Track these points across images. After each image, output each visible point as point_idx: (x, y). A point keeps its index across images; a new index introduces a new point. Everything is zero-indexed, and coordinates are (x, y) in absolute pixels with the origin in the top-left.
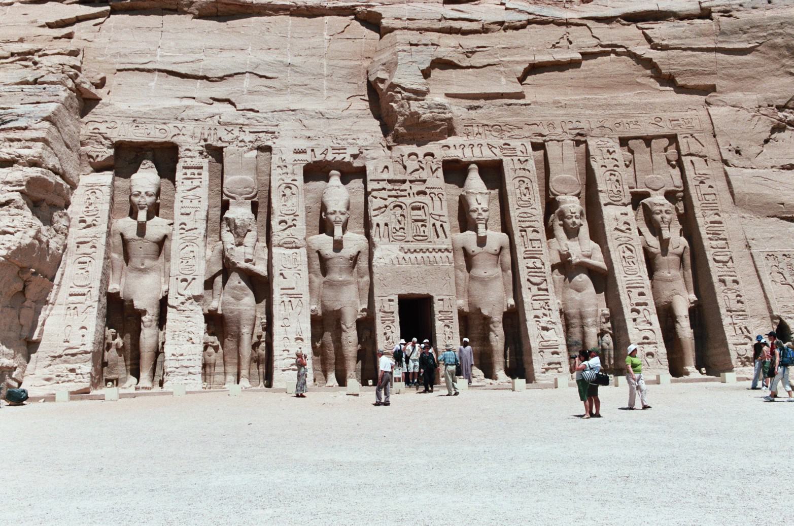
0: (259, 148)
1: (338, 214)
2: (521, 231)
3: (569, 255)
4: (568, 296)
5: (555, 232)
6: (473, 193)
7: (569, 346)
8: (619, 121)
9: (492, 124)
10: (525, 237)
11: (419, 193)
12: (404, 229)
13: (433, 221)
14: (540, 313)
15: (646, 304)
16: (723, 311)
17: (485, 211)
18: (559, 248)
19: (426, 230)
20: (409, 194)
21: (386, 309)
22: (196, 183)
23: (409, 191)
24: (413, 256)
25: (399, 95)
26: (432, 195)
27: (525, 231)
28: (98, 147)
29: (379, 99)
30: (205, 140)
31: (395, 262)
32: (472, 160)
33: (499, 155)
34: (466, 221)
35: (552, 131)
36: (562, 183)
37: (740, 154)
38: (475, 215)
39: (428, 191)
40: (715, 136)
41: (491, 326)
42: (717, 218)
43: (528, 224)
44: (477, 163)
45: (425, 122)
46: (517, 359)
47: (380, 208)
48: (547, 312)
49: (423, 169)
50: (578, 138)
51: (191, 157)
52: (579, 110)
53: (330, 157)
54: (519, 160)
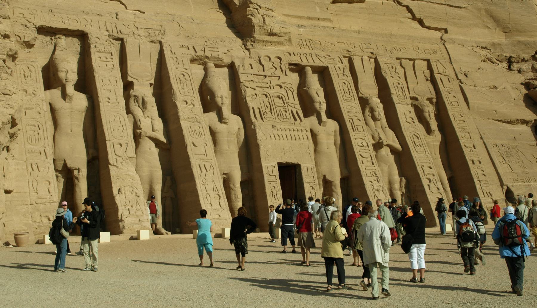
0: (153, 42)
1: (224, 98)
3: (380, 139)
8: (394, 46)
12: (271, 113)
13: (290, 108)
14: (372, 179)
15: (434, 175)
16: (476, 180)
19: (287, 114)
21: (271, 173)
22: (110, 65)
24: (284, 133)
25: (256, 11)
26: (287, 89)
28: (23, 28)
29: (231, 12)
30: (107, 31)
37: (467, 76)
39: (283, 85)
40: (451, 63)
42: (462, 119)
43: (353, 114)
44: (312, 67)
47: (253, 95)
50: (371, 55)
51: (100, 44)
53: (208, 54)
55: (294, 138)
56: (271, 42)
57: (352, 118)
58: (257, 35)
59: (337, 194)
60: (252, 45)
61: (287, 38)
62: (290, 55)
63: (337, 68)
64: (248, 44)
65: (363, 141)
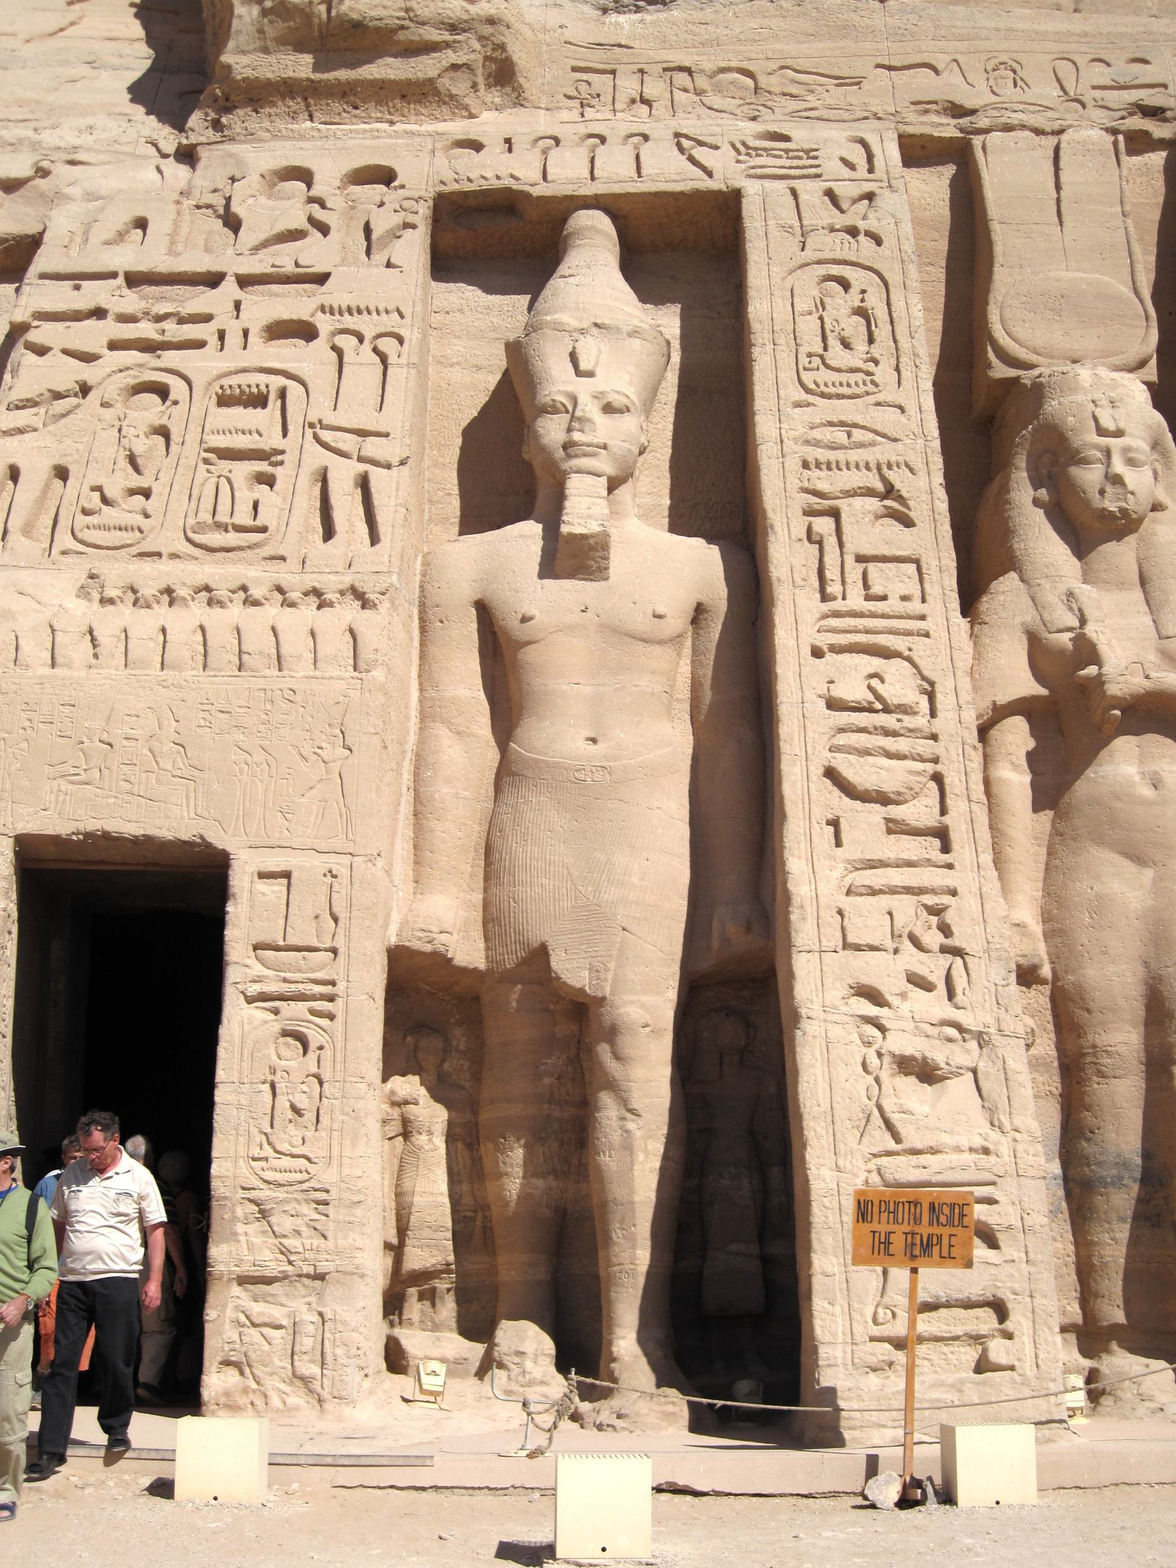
2: (810, 512)
4: (1083, 888)
5: (1018, 546)
6: (559, 328)
7: (1079, 1191)
9: (709, 65)
10: (831, 542)
11: (280, 330)
14: (885, 972)
17: (608, 409)
18: (1029, 616)
20: (222, 335)
23: (224, 318)
24: (144, 624)
26: (347, 343)
27: (835, 514)
31: (35, 650)
32: (590, 190)
33: (726, 171)
34: (507, 466)
35: (1008, 92)
36: (1059, 312)
38: (551, 430)
39: (324, 324)
41: (603, 1050)
44: (615, 207)
45: (358, 26)
46: (765, 1260)
48: (933, 967)
49: (324, 229)
50: (1137, 123)
52: (1144, 20)
54: (830, 194)
55: (223, 655)
56: (353, 96)
57: (842, 504)
58: (242, 59)
59: (624, 1102)
60: (217, 125)
61: (470, 51)
62: (477, 146)
63: (811, 192)
64: (195, 119)
65: (895, 669)
